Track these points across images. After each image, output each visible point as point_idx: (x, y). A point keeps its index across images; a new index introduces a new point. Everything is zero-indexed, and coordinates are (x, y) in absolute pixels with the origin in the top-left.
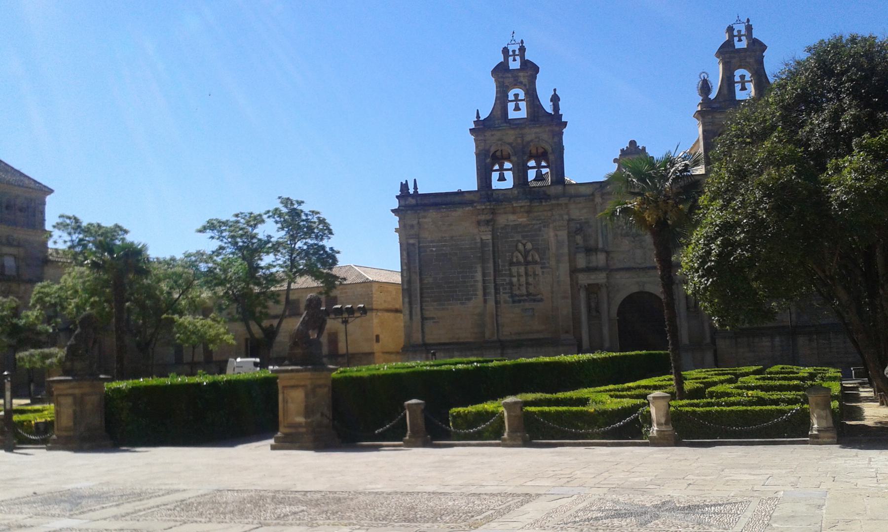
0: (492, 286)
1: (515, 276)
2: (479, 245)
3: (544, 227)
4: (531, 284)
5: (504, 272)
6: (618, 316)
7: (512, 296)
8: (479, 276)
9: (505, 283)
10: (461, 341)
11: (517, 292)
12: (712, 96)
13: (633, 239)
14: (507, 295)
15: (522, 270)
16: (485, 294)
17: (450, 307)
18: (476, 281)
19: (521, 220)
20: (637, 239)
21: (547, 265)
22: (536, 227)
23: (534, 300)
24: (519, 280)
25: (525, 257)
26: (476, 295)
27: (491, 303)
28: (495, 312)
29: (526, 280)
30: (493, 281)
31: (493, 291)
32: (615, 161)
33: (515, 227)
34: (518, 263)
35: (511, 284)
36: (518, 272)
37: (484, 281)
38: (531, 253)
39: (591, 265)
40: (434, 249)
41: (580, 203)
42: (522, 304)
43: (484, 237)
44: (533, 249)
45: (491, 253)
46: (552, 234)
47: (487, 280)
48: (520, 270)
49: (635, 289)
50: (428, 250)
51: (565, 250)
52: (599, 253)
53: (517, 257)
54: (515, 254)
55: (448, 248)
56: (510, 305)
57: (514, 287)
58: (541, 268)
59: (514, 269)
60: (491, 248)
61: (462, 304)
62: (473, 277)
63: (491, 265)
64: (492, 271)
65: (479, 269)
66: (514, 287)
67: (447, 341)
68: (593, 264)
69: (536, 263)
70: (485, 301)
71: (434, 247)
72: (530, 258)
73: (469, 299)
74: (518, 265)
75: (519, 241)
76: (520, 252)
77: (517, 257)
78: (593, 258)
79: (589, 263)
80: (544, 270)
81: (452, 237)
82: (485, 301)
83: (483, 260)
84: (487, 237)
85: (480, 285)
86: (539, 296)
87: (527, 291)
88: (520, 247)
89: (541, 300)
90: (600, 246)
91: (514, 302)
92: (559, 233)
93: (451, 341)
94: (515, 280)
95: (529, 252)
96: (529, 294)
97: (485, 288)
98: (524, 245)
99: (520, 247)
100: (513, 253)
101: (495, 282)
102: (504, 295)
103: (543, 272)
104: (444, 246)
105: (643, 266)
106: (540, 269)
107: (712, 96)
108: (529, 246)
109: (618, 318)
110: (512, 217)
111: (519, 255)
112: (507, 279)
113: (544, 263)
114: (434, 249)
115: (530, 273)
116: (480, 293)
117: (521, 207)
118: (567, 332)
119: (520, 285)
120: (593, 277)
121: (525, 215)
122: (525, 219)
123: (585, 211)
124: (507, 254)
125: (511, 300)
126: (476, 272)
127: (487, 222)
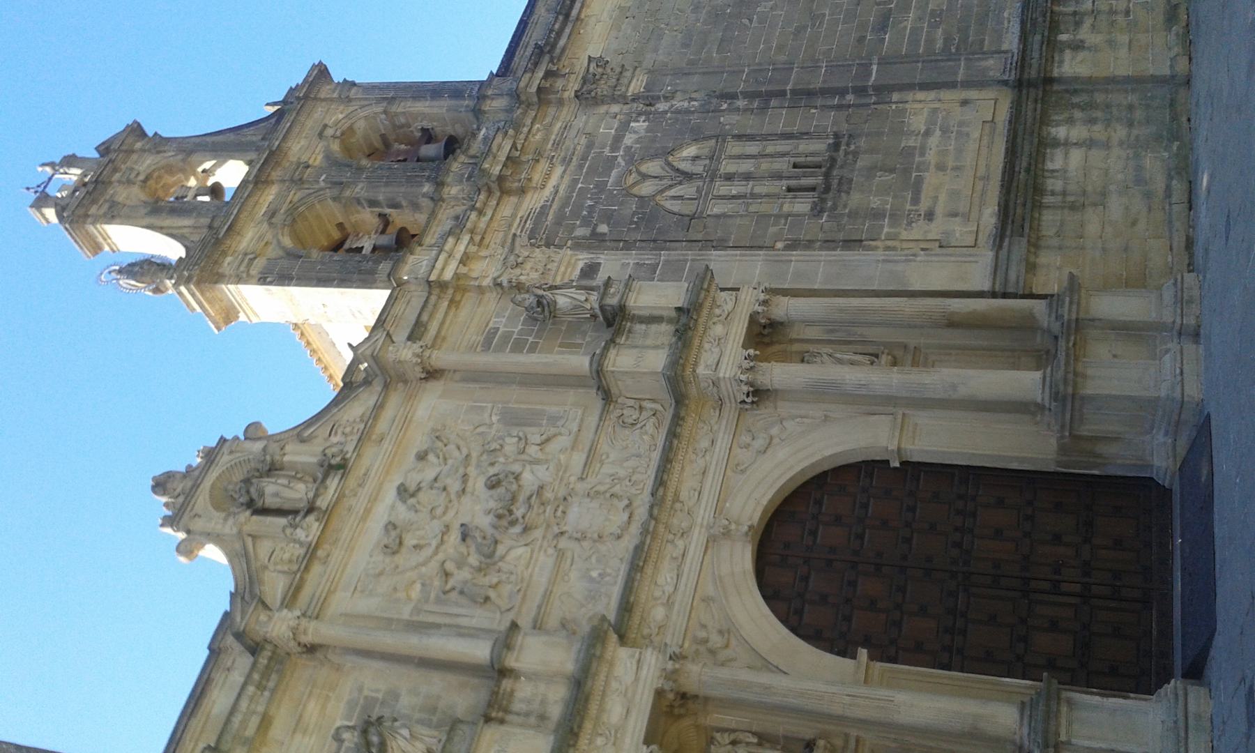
6: (854, 657)
12: (173, 250)
13: (517, 529)
20: (519, 512)
32: (186, 549)
39: (555, 712)
41: (266, 722)
49: (742, 559)
52: (511, 661)
68: (556, 697)
78: (523, 693)
79: (542, 717)
90: (480, 651)
105: (641, 512)
107: (173, 250)
109: (863, 653)
120: (614, 710)
123: (312, 708)
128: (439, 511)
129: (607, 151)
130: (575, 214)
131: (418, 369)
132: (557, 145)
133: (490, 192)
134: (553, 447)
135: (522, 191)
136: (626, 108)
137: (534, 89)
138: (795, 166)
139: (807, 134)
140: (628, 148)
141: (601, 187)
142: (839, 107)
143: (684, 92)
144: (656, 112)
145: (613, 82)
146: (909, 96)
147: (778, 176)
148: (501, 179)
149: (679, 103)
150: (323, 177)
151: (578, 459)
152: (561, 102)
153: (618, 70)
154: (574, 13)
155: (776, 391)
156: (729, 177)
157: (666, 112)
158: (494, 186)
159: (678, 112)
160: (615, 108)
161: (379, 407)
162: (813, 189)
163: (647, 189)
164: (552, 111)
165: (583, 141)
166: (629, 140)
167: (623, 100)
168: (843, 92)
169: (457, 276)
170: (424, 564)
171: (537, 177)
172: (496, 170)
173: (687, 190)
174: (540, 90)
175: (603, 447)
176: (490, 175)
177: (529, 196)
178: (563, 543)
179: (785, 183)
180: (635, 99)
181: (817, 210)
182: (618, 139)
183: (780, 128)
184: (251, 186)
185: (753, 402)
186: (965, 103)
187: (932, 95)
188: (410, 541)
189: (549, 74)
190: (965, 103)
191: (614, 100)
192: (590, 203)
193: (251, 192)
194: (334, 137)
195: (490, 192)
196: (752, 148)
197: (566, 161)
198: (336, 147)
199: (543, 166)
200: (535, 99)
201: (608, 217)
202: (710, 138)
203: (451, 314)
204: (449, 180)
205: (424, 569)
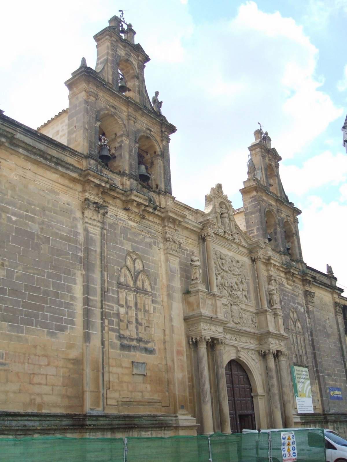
0: (97, 312)
1: (122, 306)
2: (81, 238)
3: (155, 243)
4: (141, 324)
5: (111, 294)
7: (121, 337)
8: (78, 290)
9: (112, 312)
10: (45, 411)
11: (126, 333)
14: (115, 334)
15: (131, 297)
16: (87, 324)
17: (30, 337)
18: (73, 298)
19: (131, 223)
21: (159, 299)
22: (148, 240)
23: (146, 350)
24: (127, 313)
25: (135, 279)
26: (72, 323)
27: (96, 341)
28: (101, 360)
29: (136, 315)
30: (99, 305)
31: (99, 321)
33: (125, 230)
34: (126, 287)
35: (118, 315)
36: (126, 300)
37: (86, 301)
38: (140, 277)
40: (14, 218)
42: (132, 353)
43: (91, 229)
44: (143, 271)
45: (98, 257)
46: (163, 257)
47: (92, 300)
48: (129, 299)
50: (4, 216)
51: (177, 284)
53: (125, 276)
54: (123, 271)
55: (37, 226)
56: (119, 351)
57: (121, 323)
58: (153, 301)
59: (123, 295)
60: (98, 250)
61: (52, 334)
62: (69, 290)
63: (97, 276)
64: (98, 287)
65: (79, 280)
66: (121, 323)
67: (21, 411)
69: (145, 292)
70: (87, 337)
71: (14, 214)
72: (139, 283)
73: (62, 329)
74: (127, 289)
75: (129, 254)
76: (128, 269)
77: (125, 276)
80: (156, 306)
81: (44, 209)
82: (87, 337)
83: (87, 265)
84: (95, 231)
85: (79, 307)
86: (149, 346)
87: (137, 334)
88: (129, 263)
89: (150, 351)
91: (123, 347)
92: (171, 258)
93: (30, 410)
94: (122, 311)
95: (139, 273)
96: (139, 340)
97: (87, 313)
98: (134, 261)
99: (129, 263)
100: (121, 268)
101: (102, 308)
102: (110, 333)
103: (155, 308)
104: (32, 219)
106: (150, 303)
108: (139, 266)
110: (123, 215)
111: (128, 272)
112: (115, 307)
113: (156, 294)
114: (14, 218)
115: (139, 306)
116: (79, 320)
117: (139, 204)
118: (182, 407)
119: (129, 322)
121: (138, 219)
122: (135, 225)
124: (116, 267)
125: (119, 342)
126: (75, 284)
127: (98, 207)
128: (230, 268)
129: (296, 301)
130: (285, 295)
131: (256, 257)
132: (296, 286)
133: (286, 269)
134: (244, 299)
135: (287, 279)
136: (305, 305)
137: (308, 278)
138: (301, 356)
139: (307, 358)
140: (297, 307)
141: (290, 301)
142: (313, 366)
143: (311, 321)
144: (305, 314)
145: (310, 300)
146: (317, 385)
147: (299, 352)
148: (290, 272)
149: (308, 320)
150: (280, 218)
151: (244, 307)
152: (304, 285)
153: (313, 301)
154: (321, 286)
155: (266, 360)
156: (297, 338)
157: (305, 317)
158: (288, 270)
159: (306, 320)
160: (304, 302)
161: (244, 247)
162: (298, 362)
163: (291, 314)
164: (301, 283)
165: (297, 294)
166: (299, 307)
167: (307, 304)
168: (316, 366)
169: (271, 263)
170: (220, 267)
171: (290, 282)
172: (292, 271)
173: (293, 326)
174: (307, 279)
175: (247, 313)
176: (290, 269)
177: (285, 280)
178: (229, 306)
179: (298, 354)
180: (307, 307)
181: (294, 363)
182: (298, 303)
183: (308, 350)
184: (276, 198)
185: (262, 354)
186: (318, 400)
187: (318, 391)
188: (223, 261)
189: (310, 281)
190: (318, 400)
191: (306, 301)
192: (287, 298)
193: (275, 198)
194: (287, 219)
195: (286, 269)
196: (303, 344)
197: (293, 290)
198: (285, 220)
199: (292, 283)
200: (305, 278)
201: (285, 304)
202: (303, 331)
203: (262, 263)
204: (286, 256)
205: (219, 267)
